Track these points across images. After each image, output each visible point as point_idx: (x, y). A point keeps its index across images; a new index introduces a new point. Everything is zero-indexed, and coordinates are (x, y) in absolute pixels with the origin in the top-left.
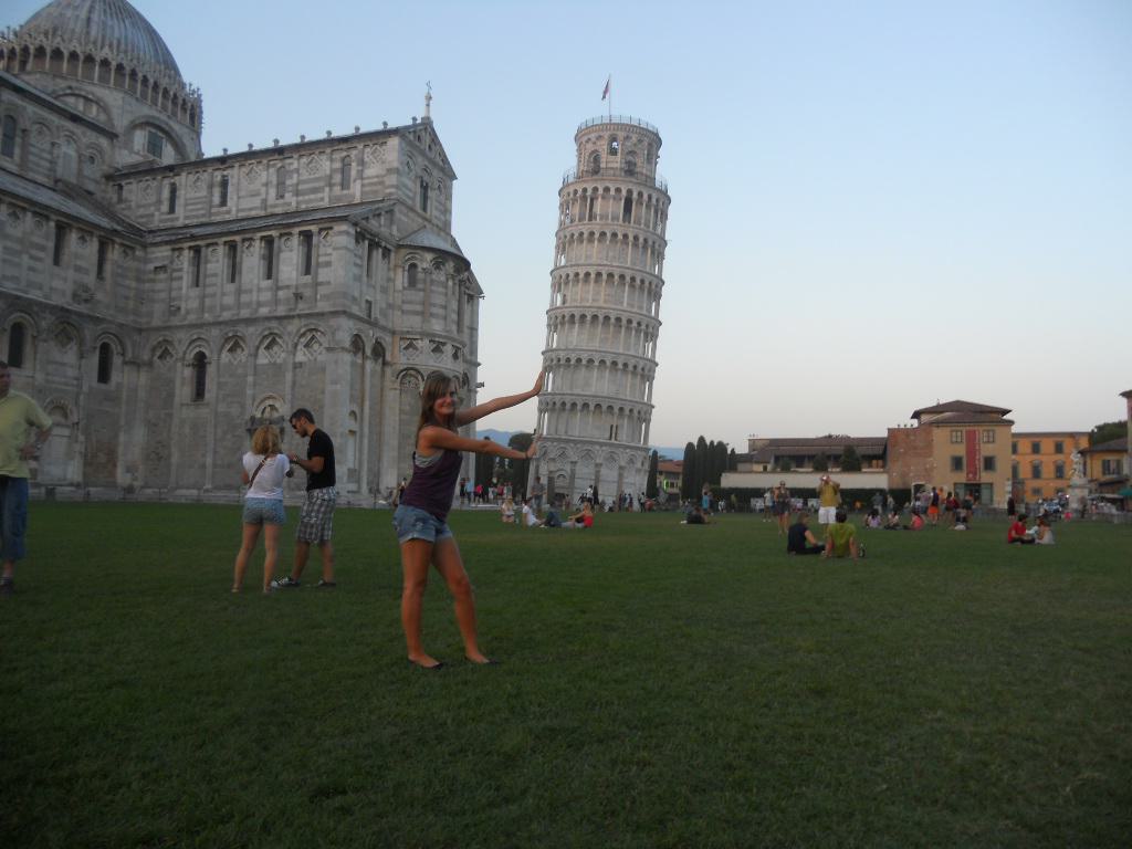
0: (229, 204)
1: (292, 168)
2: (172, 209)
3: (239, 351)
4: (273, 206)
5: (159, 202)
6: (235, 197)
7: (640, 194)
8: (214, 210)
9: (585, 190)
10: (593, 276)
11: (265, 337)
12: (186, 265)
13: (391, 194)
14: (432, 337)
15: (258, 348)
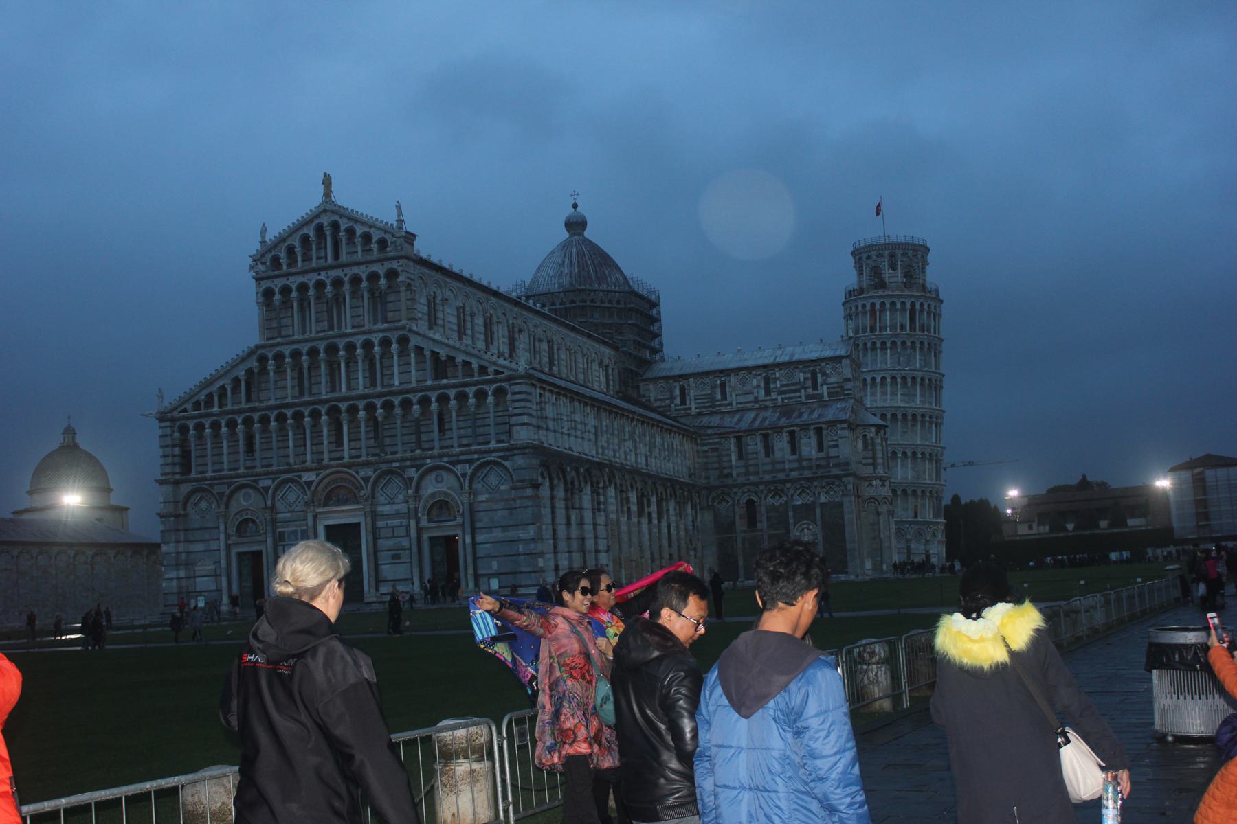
0: (729, 399)
1: (774, 376)
2: (683, 402)
3: (777, 497)
4: (762, 401)
5: (672, 398)
6: (734, 396)
7: (922, 305)
8: (717, 403)
9: (873, 305)
10: (889, 380)
11: (796, 489)
12: (732, 446)
13: (849, 394)
14: (880, 478)
15: (792, 496)
